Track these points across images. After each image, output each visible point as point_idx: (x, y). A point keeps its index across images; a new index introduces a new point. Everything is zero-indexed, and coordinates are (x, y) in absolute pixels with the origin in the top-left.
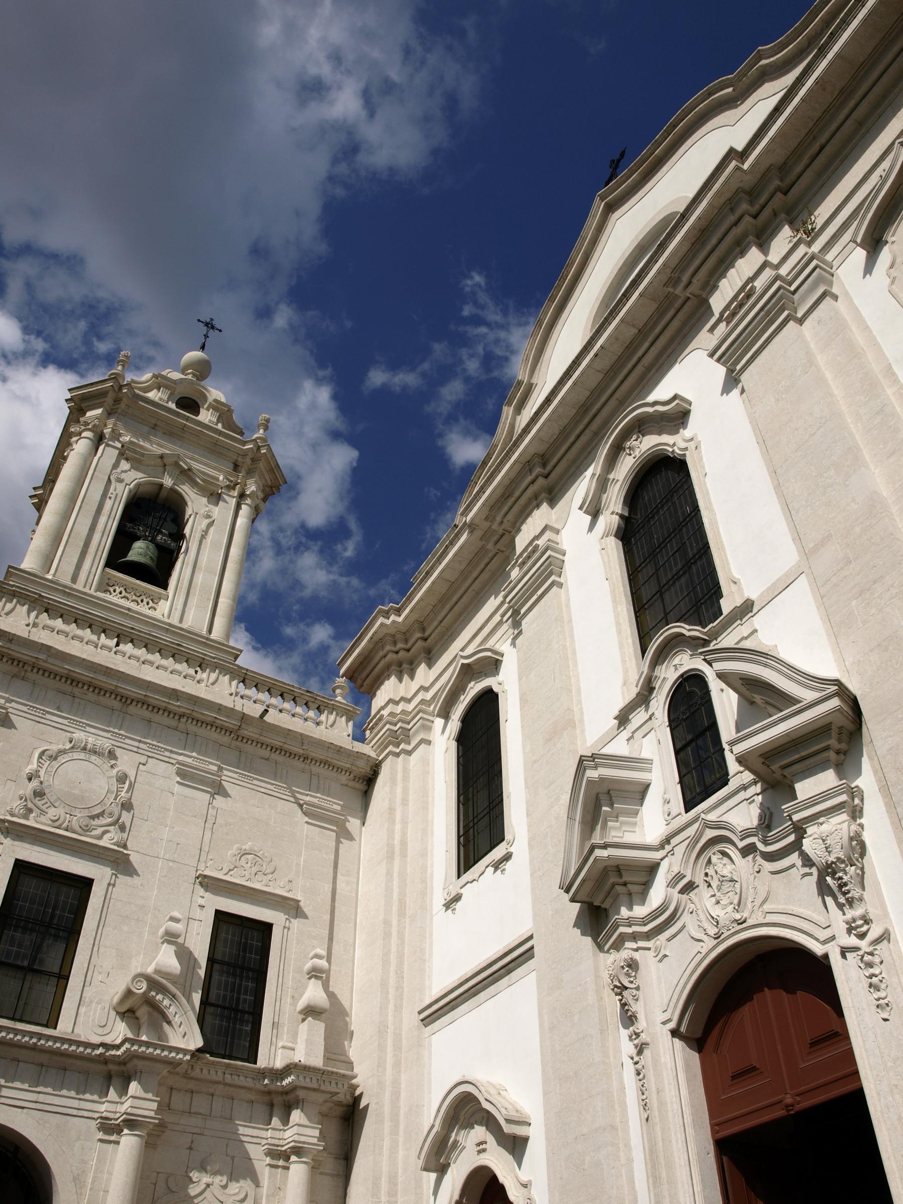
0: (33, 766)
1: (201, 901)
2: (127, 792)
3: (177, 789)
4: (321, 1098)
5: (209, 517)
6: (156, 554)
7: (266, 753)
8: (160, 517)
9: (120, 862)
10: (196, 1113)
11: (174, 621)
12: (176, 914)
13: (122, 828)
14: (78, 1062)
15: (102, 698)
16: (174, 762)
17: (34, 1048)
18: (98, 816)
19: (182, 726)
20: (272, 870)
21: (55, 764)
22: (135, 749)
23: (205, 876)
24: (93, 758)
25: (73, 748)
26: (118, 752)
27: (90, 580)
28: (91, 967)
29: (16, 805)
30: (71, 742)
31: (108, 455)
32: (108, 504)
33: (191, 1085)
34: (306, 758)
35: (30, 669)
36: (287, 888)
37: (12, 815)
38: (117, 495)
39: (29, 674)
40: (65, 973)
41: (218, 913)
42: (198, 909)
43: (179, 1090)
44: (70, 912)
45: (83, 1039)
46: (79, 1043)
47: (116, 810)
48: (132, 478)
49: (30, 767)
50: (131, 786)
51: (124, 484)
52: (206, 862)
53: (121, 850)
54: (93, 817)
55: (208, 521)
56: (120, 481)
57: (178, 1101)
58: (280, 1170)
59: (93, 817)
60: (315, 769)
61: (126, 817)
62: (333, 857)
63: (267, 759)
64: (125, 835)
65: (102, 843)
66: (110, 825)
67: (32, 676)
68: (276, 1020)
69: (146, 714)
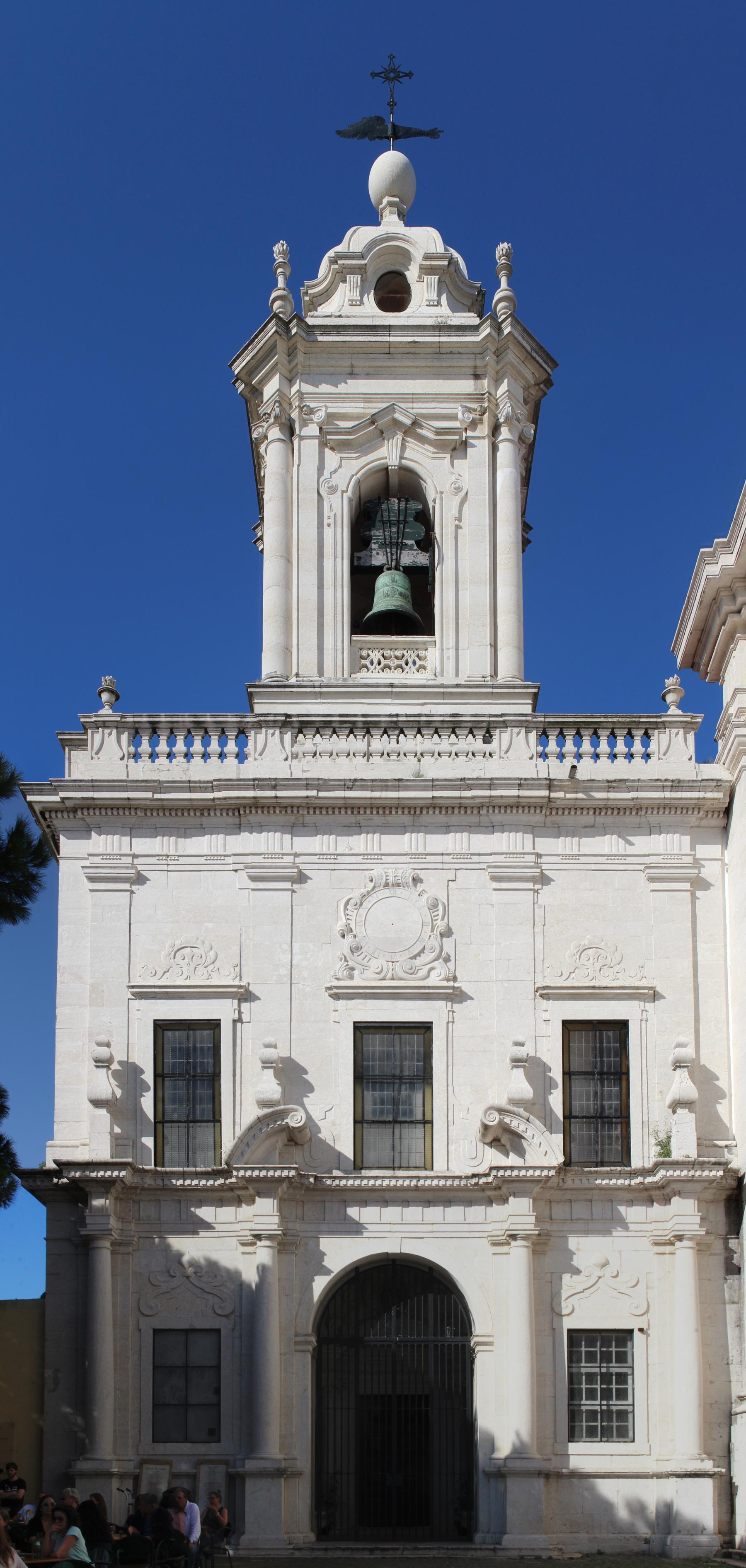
0: (343, 921)
1: (545, 1016)
2: (443, 919)
3: (497, 897)
4: (698, 1187)
5: (458, 489)
6: (407, 585)
7: (588, 819)
8: (398, 521)
9: (456, 996)
10: (578, 1219)
11: (449, 678)
12: (520, 1039)
13: (447, 960)
14: (460, 1194)
15: (389, 818)
16: (484, 866)
17: (416, 1188)
18: (419, 954)
19: (484, 820)
20: (619, 960)
21: (363, 911)
22: (440, 866)
23: (544, 988)
24: (399, 891)
25: (374, 887)
26: (422, 874)
27: (339, 663)
28: (450, 1107)
29: (339, 967)
30: (371, 881)
31: (308, 449)
32: (328, 533)
33: (568, 1195)
34: (639, 809)
35: (306, 812)
36: (639, 976)
37: (338, 979)
38: (335, 515)
39: (308, 819)
40: (428, 1118)
41: (566, 1024)
42: (544, 1024)
43: (558, 1202)
44: (418, 1061)
45: (456, 1174)
46: (454, 1178)
47: (435, 942)
48: (348, 472)
49: (339, 923)
50: (446, 910)
51: (339, 493)
52: (542, 972)
53: (451, 984)
54: (414, 957)
55: (457, 499)
56: (333, 490)
57: (560, 1211)
58: (667, 1256)
59: (414, 957)
60: (653, 819)
61: (448, 943)
62: (690, 924)
63: (593, 826)
64: (451, 965)
65: (429, 982)
66: (434, 961)
67: (309, 819)
68: (645, 1119)
69: (442, 818)
